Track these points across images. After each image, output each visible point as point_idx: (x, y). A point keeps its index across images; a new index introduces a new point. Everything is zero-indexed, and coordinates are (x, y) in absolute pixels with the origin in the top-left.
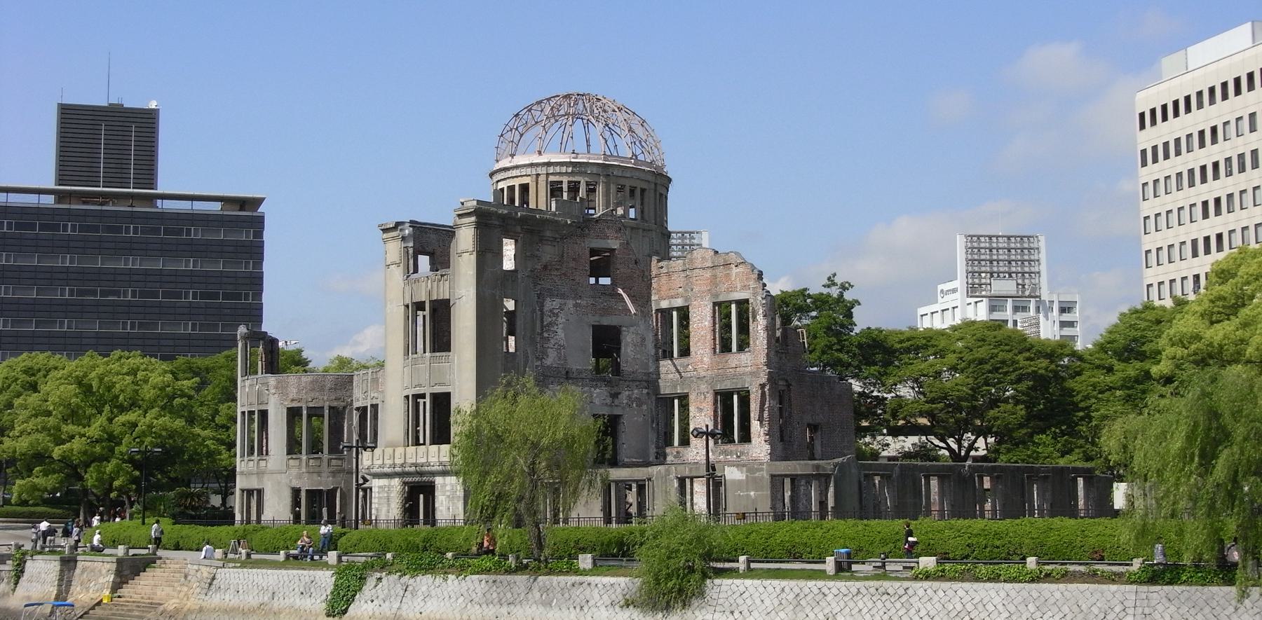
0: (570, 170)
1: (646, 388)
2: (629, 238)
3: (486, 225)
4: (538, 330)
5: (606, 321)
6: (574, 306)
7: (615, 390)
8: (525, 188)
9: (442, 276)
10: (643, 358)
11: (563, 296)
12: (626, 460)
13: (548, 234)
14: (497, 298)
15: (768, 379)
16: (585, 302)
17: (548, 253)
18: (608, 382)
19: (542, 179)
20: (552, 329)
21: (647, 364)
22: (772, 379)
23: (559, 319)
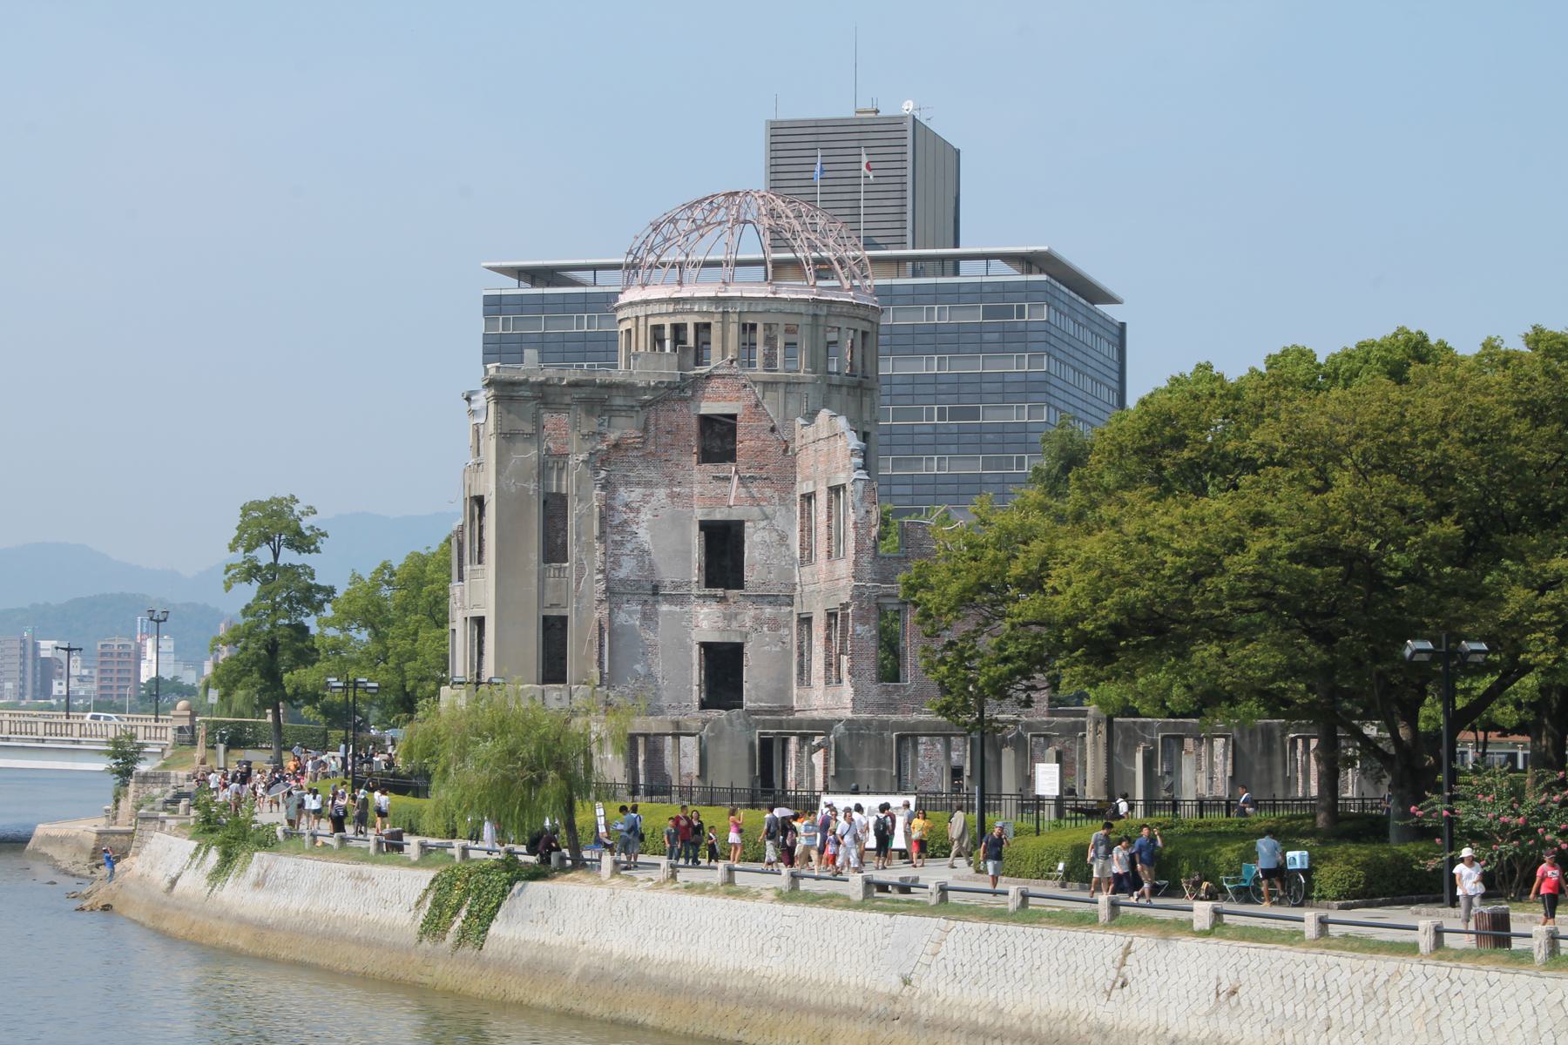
0: (671, 308)
1: (789, 605)
2: (760, 396)
3: (511, 398)
4: (596, 532)
5: (718, 516)
6: (668, 496)
7: (733, 609)
8: (629, 331)
9: (479, 465)
10: (784, 563)
11: (648, 484)
12: (749, 704)
13: (618, 401)
14: (531, 493)
15: (852, 597)
16: (687, 490)
17: (623, 429)
18: (721, 598)
19: (642, 321)
20: (629, 529)
21: (792, 571)
22: (858, 594)
23: (642, 516)
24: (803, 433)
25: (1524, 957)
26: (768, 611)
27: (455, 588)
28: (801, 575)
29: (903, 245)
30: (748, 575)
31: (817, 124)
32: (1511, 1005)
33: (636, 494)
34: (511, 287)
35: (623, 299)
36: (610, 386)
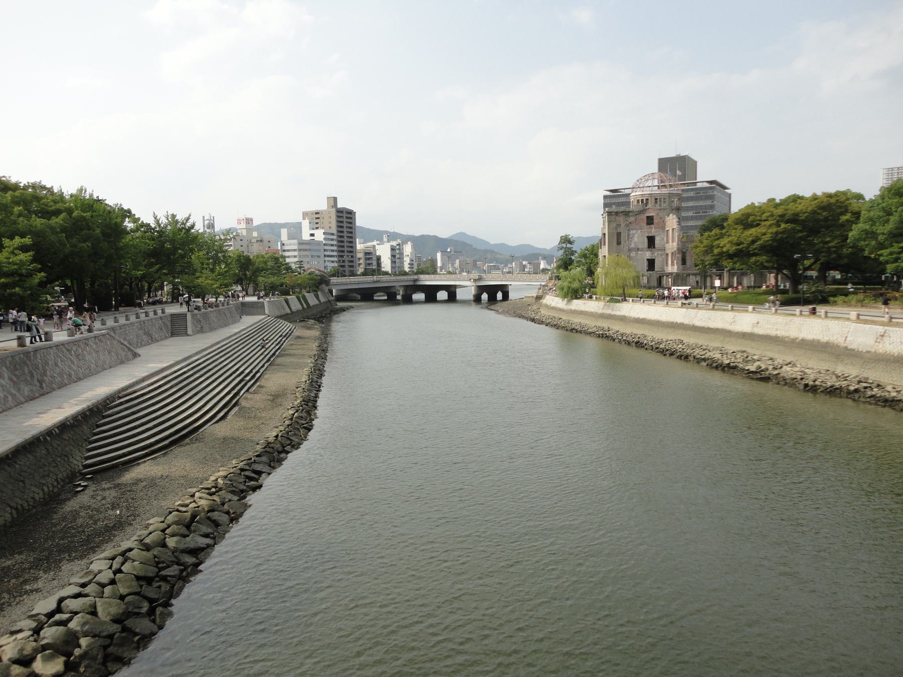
5: (650, 235)
11: (637, 230)
17: (632, 219)
22: (678, 249)
24: (667, 219)
25: (820, 316)
26: (660, 253)
27: (600, 250)
28: (667, 246)
29: (685, 181)
30: (656, 246)
31: (668, 158)
32: (816, 326)
33: (634, 231)
34: (608, 193)
35: (631, 195)
36: (629, 212)
